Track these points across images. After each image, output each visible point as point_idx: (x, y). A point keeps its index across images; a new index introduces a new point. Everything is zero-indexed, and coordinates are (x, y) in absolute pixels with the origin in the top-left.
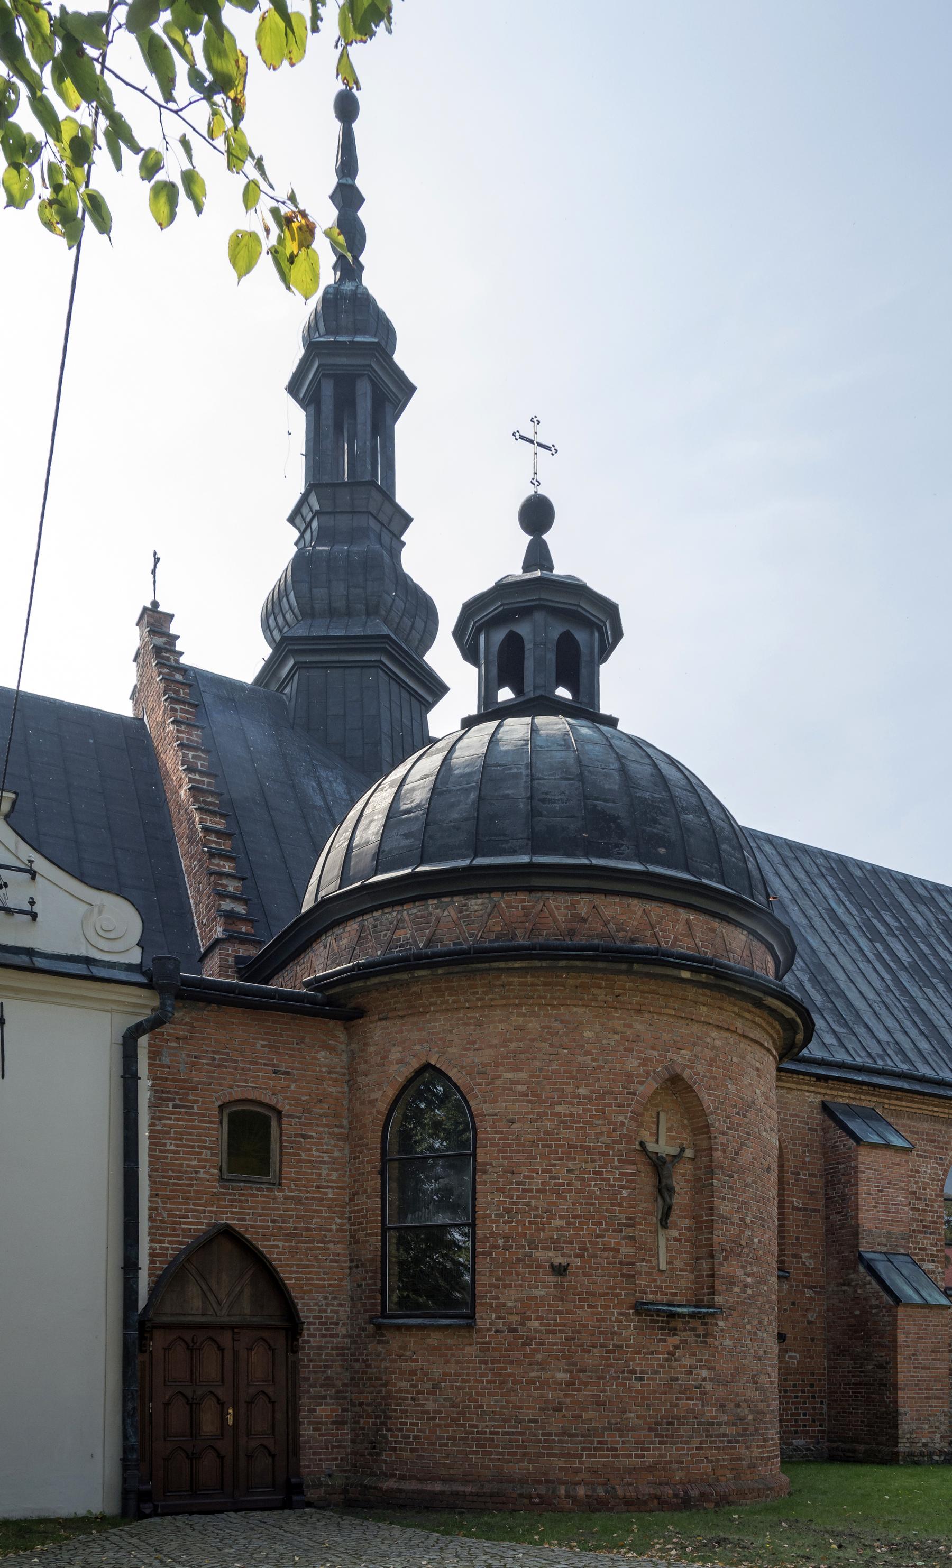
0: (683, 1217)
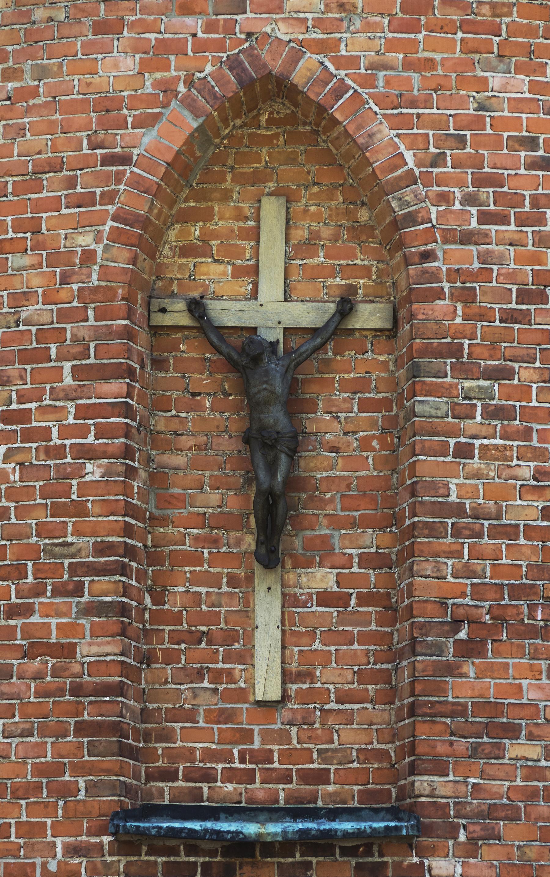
0: (353, 524)
